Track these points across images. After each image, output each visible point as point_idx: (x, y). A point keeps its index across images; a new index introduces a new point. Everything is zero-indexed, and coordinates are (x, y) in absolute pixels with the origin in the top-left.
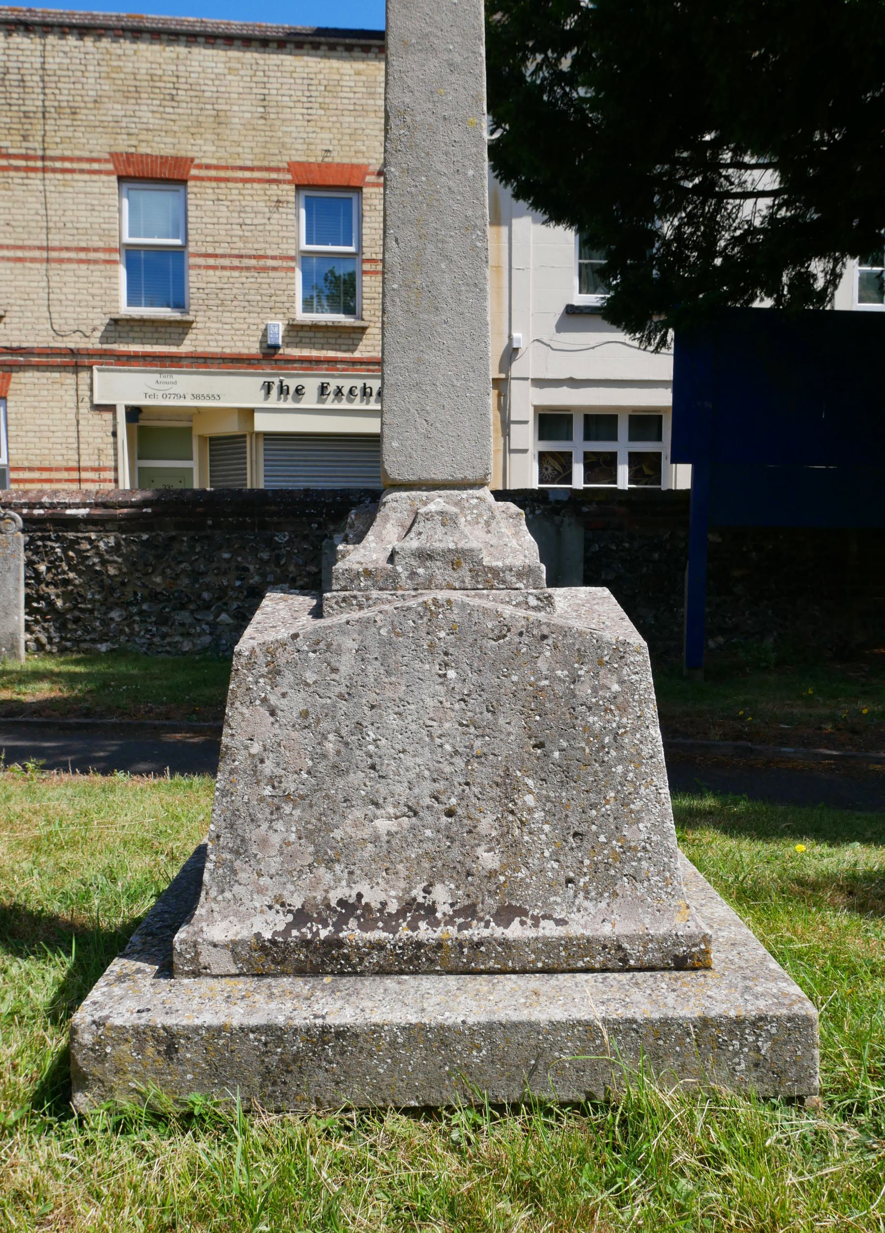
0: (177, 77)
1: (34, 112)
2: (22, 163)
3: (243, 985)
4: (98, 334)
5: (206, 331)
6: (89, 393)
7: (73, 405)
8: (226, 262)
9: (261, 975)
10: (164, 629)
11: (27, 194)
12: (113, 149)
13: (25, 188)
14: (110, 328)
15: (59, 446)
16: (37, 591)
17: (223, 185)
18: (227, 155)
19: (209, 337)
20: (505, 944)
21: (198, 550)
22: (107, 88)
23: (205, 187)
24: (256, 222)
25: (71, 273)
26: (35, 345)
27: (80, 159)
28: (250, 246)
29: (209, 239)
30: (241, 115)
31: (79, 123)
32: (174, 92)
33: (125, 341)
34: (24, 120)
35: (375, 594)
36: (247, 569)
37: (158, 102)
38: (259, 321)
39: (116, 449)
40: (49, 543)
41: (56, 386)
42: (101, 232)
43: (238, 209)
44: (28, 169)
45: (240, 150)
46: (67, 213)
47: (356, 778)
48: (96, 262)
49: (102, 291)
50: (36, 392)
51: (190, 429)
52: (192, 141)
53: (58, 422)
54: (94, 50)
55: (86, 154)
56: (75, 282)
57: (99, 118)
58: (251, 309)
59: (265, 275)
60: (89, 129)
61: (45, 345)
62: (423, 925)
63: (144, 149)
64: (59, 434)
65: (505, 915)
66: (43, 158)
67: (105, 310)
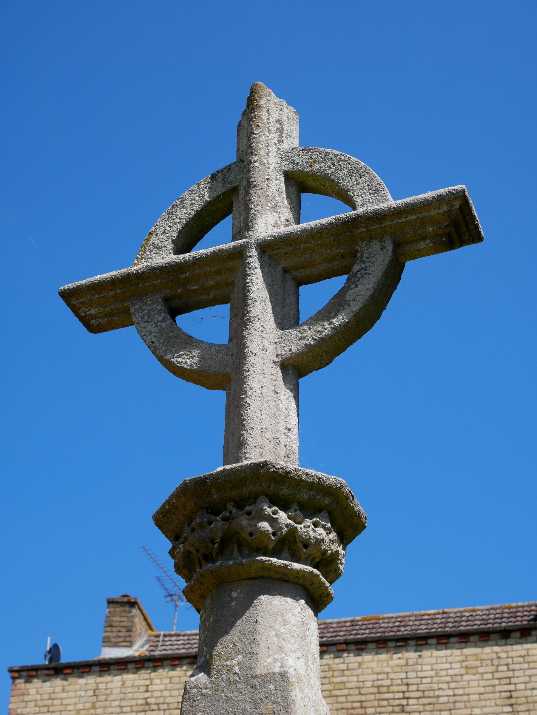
0: (407, 685)
32: (404, 702)
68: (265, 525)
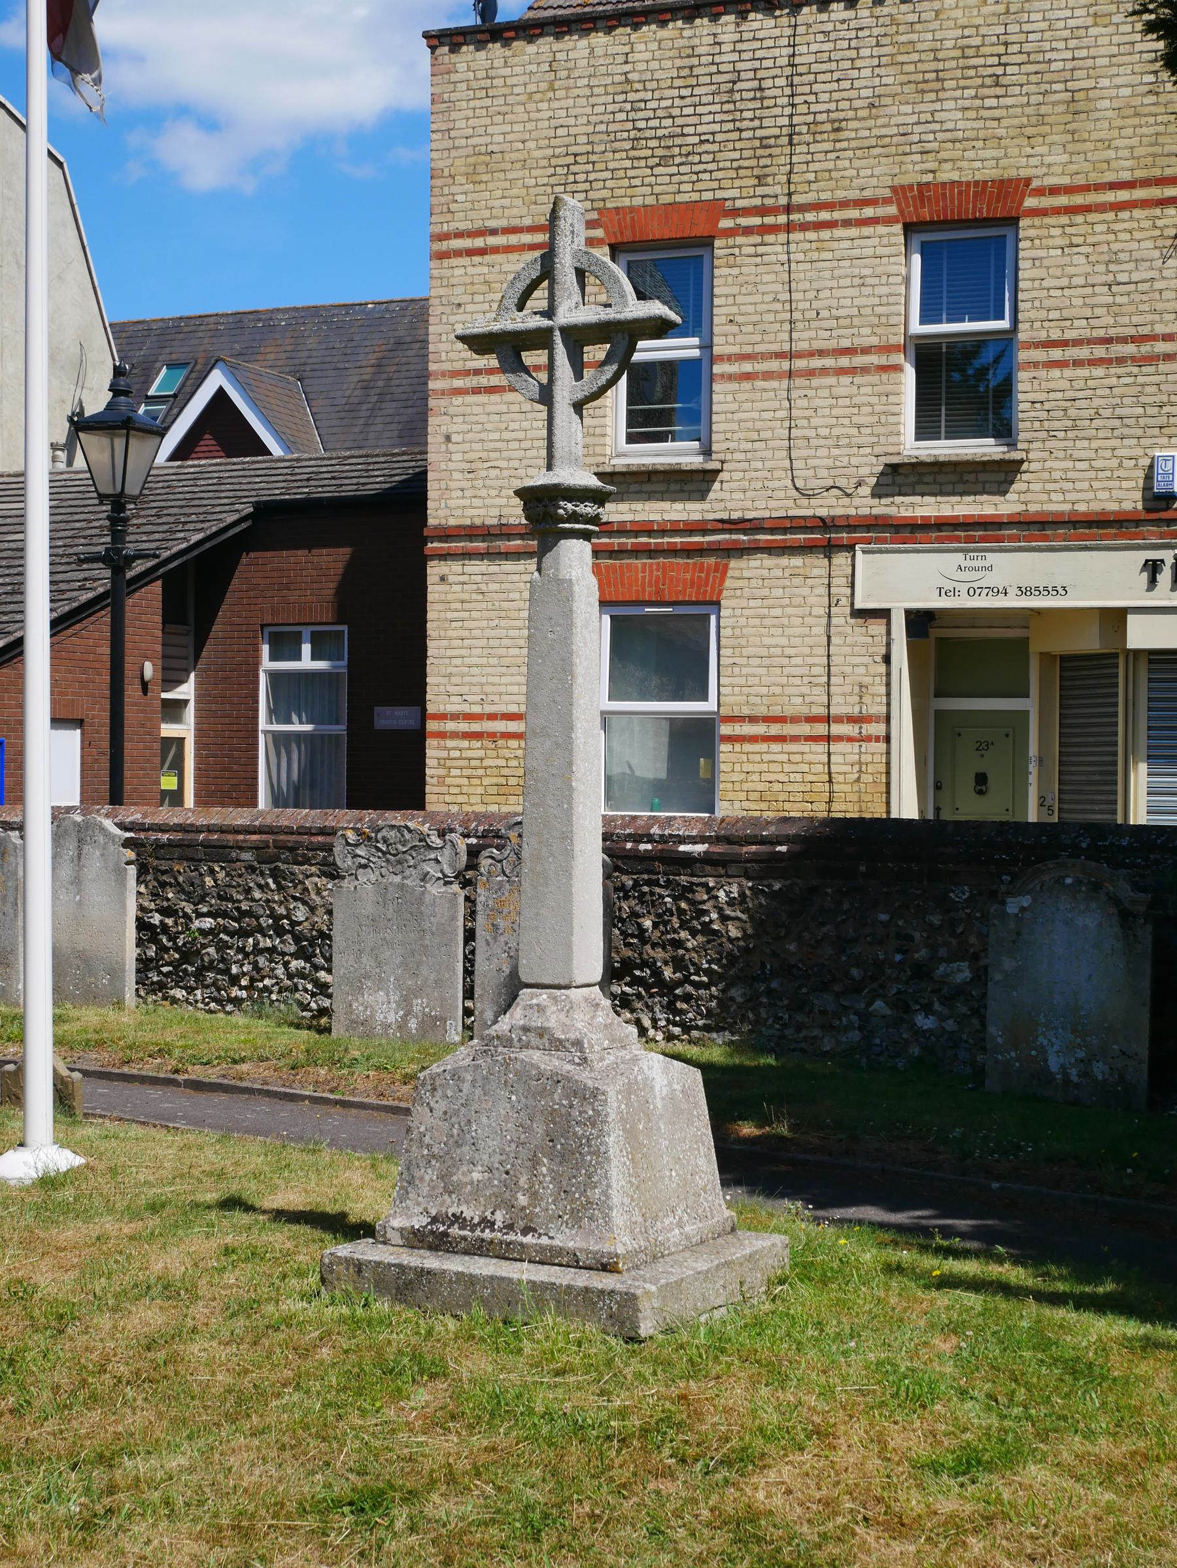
0: (1006, 44)
1: (776, 137)
2: (756, 221)
3: (405, 1250)
4: (866, 490)
5: (1046, 475)
6: (849, 591)
7: (822, 611)
8: (1083, 353)
9: (413, 1248)
10: (801, 1018)
11: (761, 269)
12: (898, 181)
13: (758, 260)
14: (884, 480)
15: (797, 681)
16: (641, 954)
17: (1079, 219)
18: (1087, 166)
19: (1050, 486)
20: (521, 1244)
21: (845, 907)
22: (890, 80)
23: (1049, 227)
24: (1136, 277)
25: (826, 393)
26: (766, 514)
27: (844, 204)
28: (1126, 320)
29: (1054, 315)
30: (1113, 92)
31: (845, 144)
32: (999, 71)
33: (909, 502)
34: (760, 152)
35: (500, 1049)
36: (910, 938)
37: (972, 92)
38: (1140, 452)
39: (888, 685)
40: (657, 890)
41: (797, 581)
42: (876, 320)
43: (1106, 258)
44: (764, 230)
45: (1111, 154)
46: (822, 295)
47: (465, 1149)
48: (865, 370)
49: (875, 419)
50: (766, 592)
51: (1024, 643)
52: (1029, 150)
53: (798, 641)
54: (871, 22)
55: (854, 194)
56: (831, 407)
57: (875, 132)
58: (1126, 431)
59: (1151, 369)
60: (859, 153)
61: (782, 514)
63: (948, 175)
64: (798, 661)
65: (526, 1231)
66: (788, 209)
67: (878, 450)
68: (561, 511)
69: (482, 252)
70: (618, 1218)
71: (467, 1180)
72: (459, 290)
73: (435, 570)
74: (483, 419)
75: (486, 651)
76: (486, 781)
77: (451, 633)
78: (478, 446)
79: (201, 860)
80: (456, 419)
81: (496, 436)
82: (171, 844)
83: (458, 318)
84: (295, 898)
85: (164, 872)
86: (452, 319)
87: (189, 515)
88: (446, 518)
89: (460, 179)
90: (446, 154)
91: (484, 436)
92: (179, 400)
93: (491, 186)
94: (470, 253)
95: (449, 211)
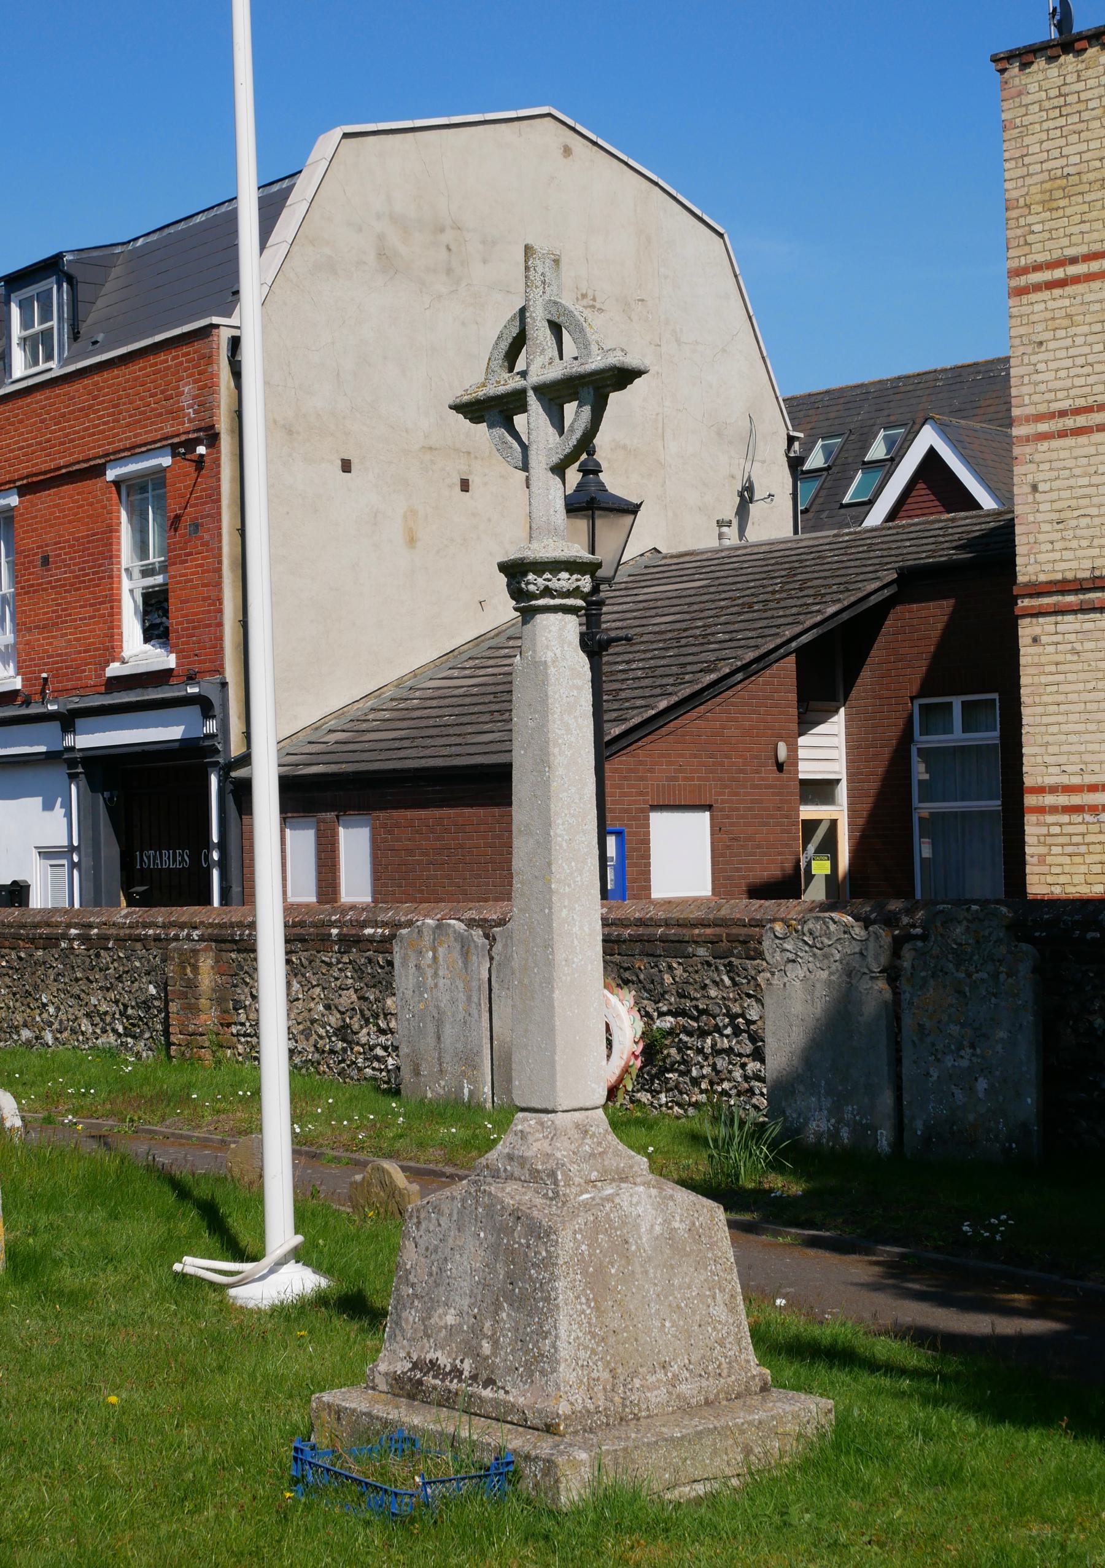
62: (455, 1381)
68: (532, 588)
69: (1062, 283)
70: (566, 1373)
71: (442, 1324)
72: (1039, 327)
73: (1026, 629)
74: (1070, 463)
75: (1084, 717)
76: (1089, 859)
77: (1046, 699)
78: (1066, 494)
79: (660, 956)
80: (1043, 467)
81: (1085, 481)
82: (633, 940)
83: (1040, 357)
84: (749, 996)
85: (626, 969)
86: (1034, 359)
87: (830, 586)
88: (1036, 574)
89: (1036, 208)
90: (1020, 182)
91: (1072, 482)
92: (892, 462)
93: (1068, 212)
94: (1051, 285)
95: (1026, 243)
